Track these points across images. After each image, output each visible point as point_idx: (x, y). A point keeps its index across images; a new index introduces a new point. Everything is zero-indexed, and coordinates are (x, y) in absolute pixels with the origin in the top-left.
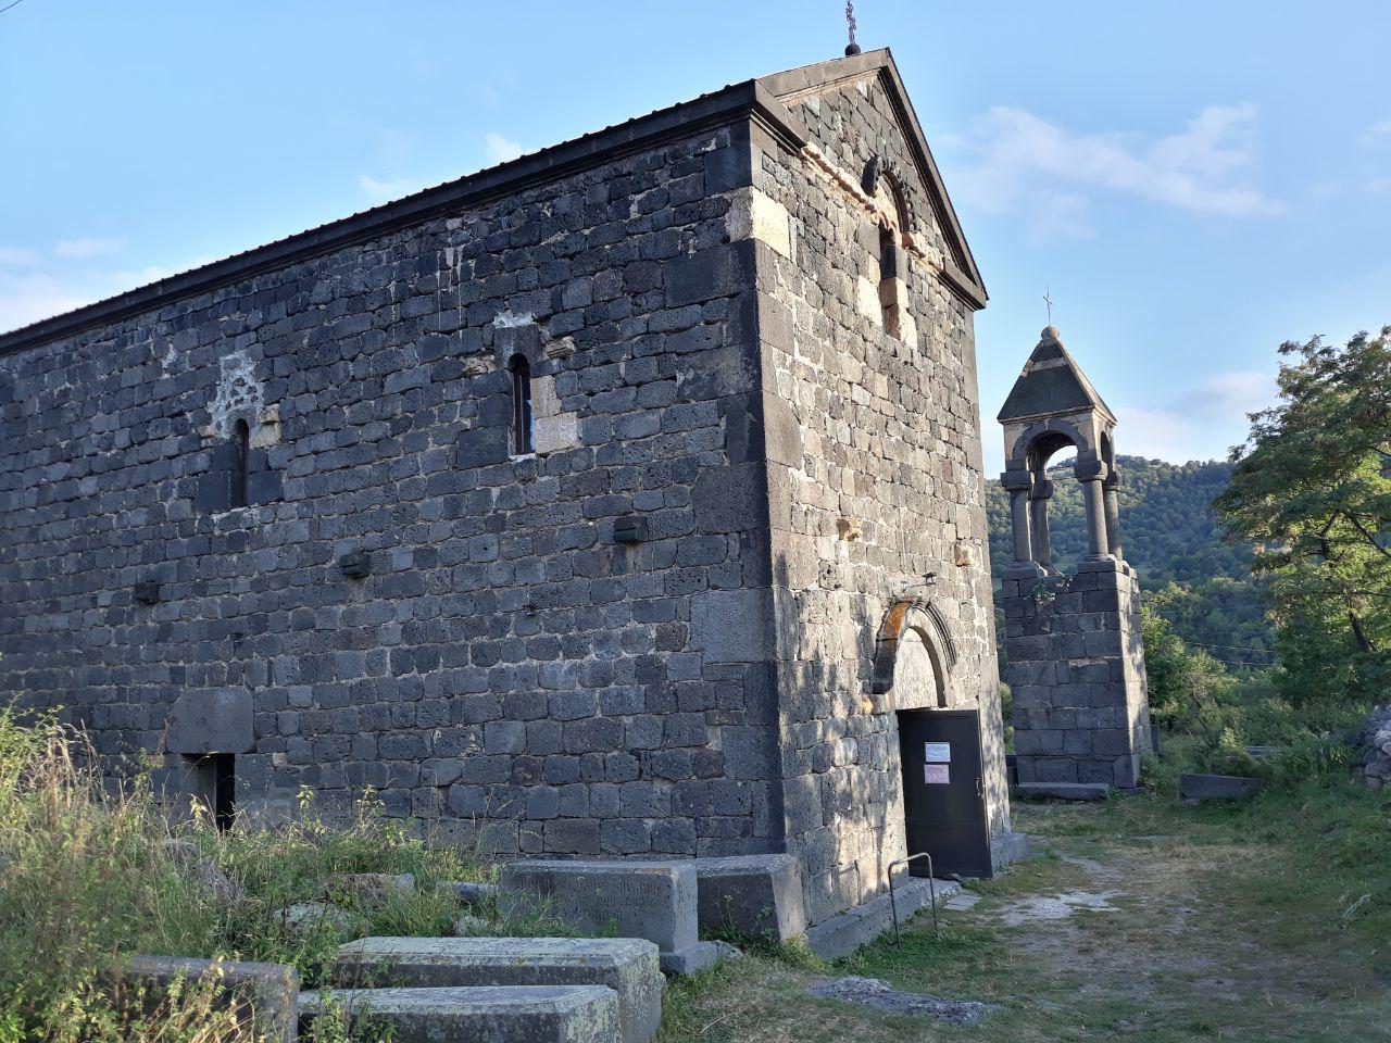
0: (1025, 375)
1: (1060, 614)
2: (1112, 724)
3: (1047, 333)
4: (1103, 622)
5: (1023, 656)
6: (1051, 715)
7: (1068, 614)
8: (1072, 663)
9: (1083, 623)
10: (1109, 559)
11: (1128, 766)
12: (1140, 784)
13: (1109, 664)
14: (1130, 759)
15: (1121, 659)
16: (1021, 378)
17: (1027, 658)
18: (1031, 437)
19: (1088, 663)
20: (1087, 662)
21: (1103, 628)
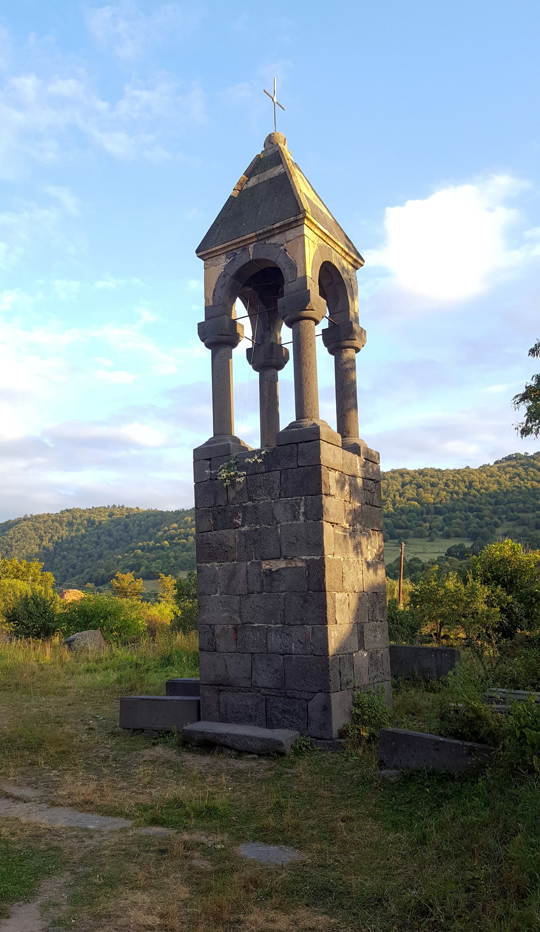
0: (236, 194)
1: (253, 501)
2: (309, 648)
3: (270, 141)
4: (302, 510)
5: (212, 557)
6: (239, 633)
7: (263, 500)
8: (265, 566)
9: (279, 510)
10: (314, 424)
11: (326, 708)
12: (343, 734)
13: (308, 566)
14: (330, 696)
15: (322, 560)
16: (231, 196)
17: (216, 559)
18: (232, 271)
19: (284, 566)
20: (282, 564)
21: (302, 518)
